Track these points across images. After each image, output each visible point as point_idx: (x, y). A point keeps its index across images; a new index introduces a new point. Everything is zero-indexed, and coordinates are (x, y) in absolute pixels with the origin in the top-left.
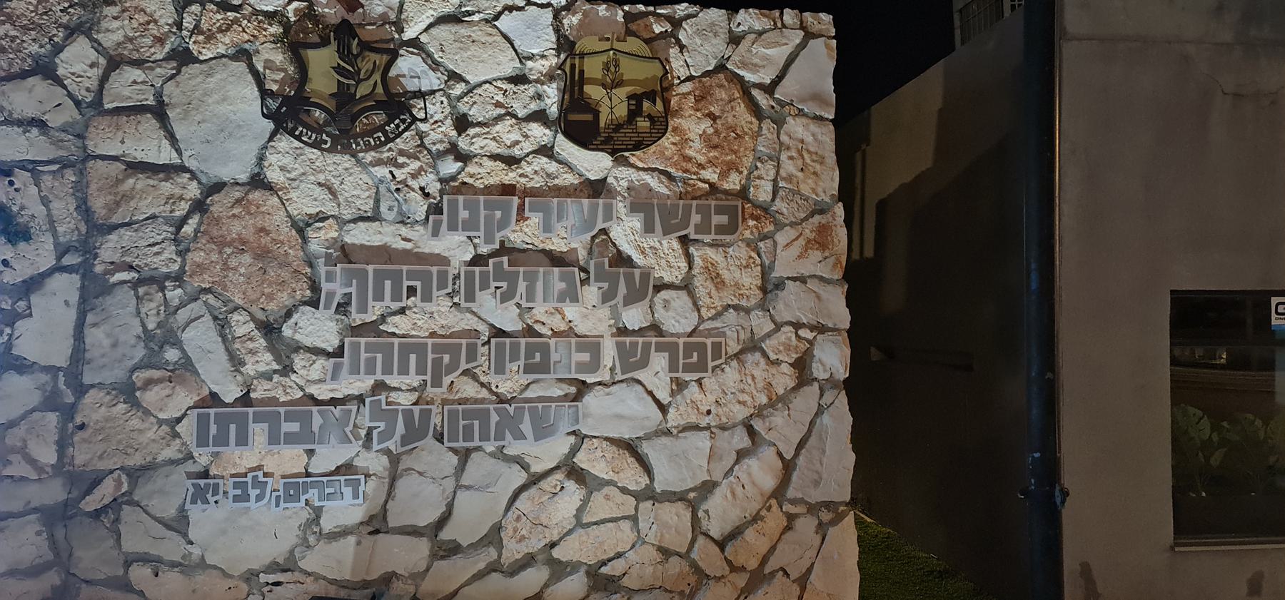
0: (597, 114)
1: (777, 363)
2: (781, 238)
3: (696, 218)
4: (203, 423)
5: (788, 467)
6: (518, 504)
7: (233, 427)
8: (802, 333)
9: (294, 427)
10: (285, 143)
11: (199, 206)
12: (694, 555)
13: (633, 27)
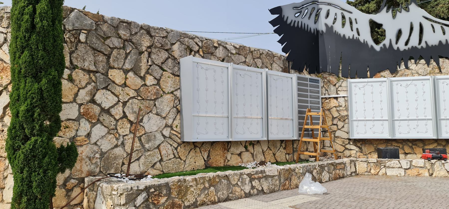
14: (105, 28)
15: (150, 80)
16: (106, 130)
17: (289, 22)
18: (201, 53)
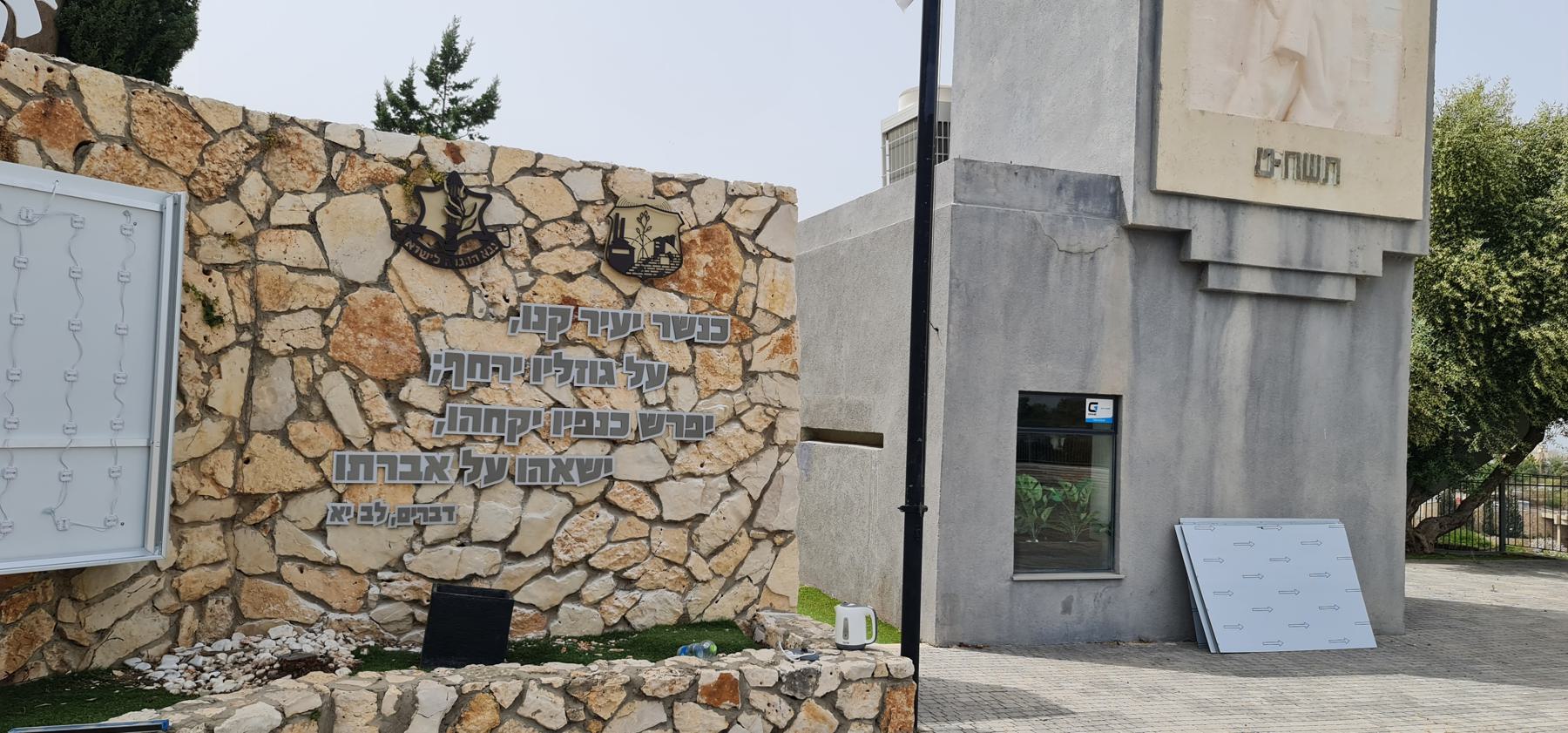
0: (632, 249)
1: (751, 431)
2: (759, 342)
3: (698, 328)
4: (341, 459)
5: (756, 504)
6: (567, 526)
7: (362, 467)
8: (770, 410)
9: (407, 468)
10: (402, 255)
11: (340, 299)
12: (689, 564)
13: (660, 187)
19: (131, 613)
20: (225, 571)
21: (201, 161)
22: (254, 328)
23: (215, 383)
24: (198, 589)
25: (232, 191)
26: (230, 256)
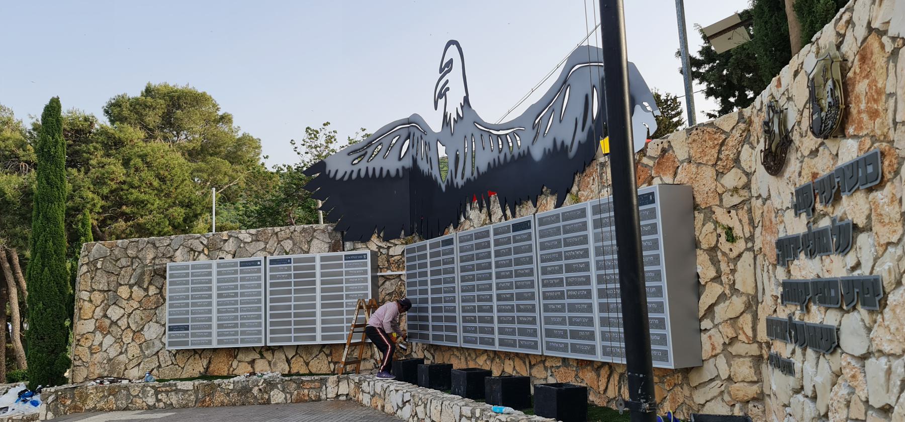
14: (116, 252)
15: (152, 290)
16: (114, 339)
17: (339, 176)
18: (206, 252)
19: (712, 399)
20: (755, 388)
21: (719, 152)
22: (751, 239)
23: (736, 275)
24: (741, 395)
25: (737, 161)
26: (736, 200)
